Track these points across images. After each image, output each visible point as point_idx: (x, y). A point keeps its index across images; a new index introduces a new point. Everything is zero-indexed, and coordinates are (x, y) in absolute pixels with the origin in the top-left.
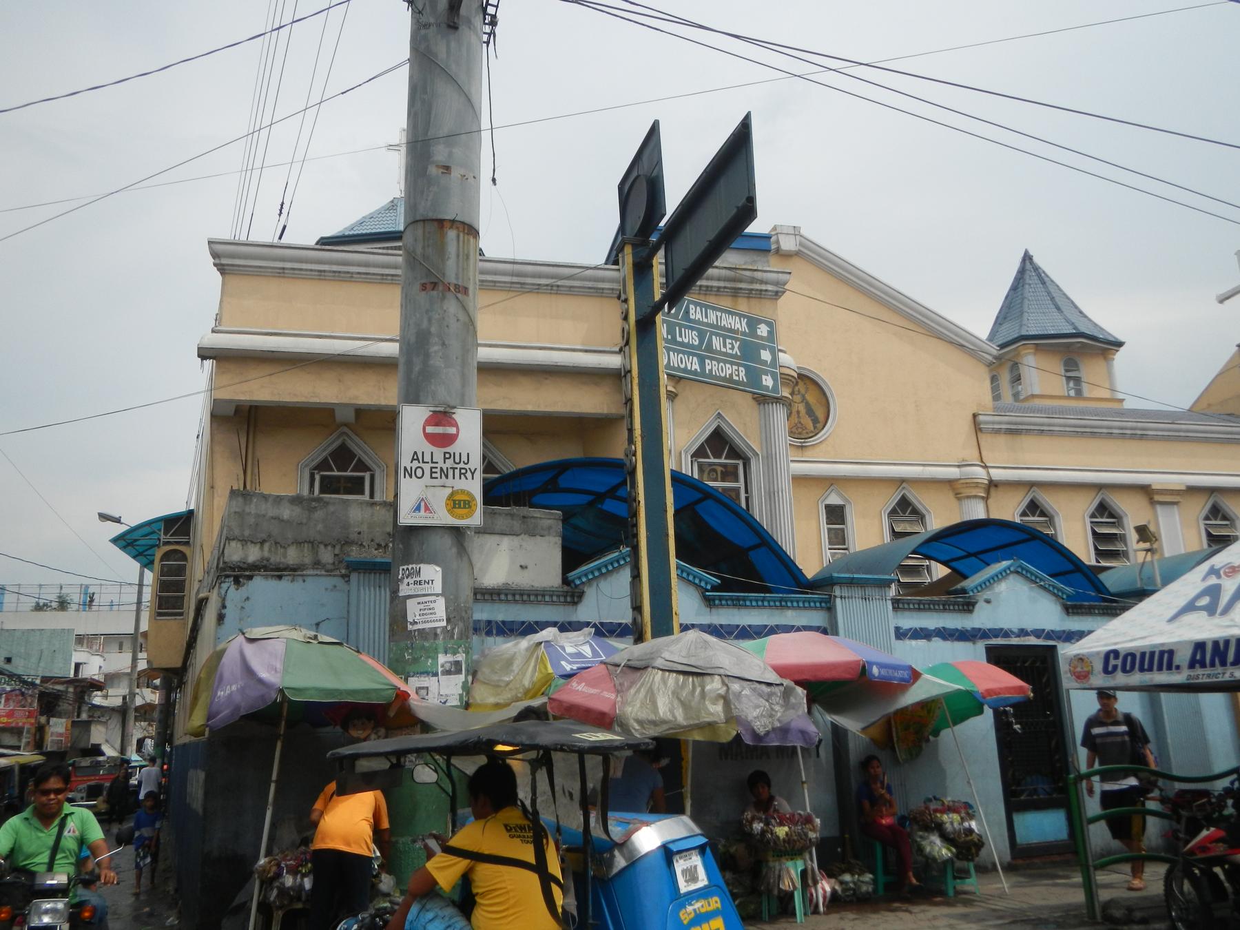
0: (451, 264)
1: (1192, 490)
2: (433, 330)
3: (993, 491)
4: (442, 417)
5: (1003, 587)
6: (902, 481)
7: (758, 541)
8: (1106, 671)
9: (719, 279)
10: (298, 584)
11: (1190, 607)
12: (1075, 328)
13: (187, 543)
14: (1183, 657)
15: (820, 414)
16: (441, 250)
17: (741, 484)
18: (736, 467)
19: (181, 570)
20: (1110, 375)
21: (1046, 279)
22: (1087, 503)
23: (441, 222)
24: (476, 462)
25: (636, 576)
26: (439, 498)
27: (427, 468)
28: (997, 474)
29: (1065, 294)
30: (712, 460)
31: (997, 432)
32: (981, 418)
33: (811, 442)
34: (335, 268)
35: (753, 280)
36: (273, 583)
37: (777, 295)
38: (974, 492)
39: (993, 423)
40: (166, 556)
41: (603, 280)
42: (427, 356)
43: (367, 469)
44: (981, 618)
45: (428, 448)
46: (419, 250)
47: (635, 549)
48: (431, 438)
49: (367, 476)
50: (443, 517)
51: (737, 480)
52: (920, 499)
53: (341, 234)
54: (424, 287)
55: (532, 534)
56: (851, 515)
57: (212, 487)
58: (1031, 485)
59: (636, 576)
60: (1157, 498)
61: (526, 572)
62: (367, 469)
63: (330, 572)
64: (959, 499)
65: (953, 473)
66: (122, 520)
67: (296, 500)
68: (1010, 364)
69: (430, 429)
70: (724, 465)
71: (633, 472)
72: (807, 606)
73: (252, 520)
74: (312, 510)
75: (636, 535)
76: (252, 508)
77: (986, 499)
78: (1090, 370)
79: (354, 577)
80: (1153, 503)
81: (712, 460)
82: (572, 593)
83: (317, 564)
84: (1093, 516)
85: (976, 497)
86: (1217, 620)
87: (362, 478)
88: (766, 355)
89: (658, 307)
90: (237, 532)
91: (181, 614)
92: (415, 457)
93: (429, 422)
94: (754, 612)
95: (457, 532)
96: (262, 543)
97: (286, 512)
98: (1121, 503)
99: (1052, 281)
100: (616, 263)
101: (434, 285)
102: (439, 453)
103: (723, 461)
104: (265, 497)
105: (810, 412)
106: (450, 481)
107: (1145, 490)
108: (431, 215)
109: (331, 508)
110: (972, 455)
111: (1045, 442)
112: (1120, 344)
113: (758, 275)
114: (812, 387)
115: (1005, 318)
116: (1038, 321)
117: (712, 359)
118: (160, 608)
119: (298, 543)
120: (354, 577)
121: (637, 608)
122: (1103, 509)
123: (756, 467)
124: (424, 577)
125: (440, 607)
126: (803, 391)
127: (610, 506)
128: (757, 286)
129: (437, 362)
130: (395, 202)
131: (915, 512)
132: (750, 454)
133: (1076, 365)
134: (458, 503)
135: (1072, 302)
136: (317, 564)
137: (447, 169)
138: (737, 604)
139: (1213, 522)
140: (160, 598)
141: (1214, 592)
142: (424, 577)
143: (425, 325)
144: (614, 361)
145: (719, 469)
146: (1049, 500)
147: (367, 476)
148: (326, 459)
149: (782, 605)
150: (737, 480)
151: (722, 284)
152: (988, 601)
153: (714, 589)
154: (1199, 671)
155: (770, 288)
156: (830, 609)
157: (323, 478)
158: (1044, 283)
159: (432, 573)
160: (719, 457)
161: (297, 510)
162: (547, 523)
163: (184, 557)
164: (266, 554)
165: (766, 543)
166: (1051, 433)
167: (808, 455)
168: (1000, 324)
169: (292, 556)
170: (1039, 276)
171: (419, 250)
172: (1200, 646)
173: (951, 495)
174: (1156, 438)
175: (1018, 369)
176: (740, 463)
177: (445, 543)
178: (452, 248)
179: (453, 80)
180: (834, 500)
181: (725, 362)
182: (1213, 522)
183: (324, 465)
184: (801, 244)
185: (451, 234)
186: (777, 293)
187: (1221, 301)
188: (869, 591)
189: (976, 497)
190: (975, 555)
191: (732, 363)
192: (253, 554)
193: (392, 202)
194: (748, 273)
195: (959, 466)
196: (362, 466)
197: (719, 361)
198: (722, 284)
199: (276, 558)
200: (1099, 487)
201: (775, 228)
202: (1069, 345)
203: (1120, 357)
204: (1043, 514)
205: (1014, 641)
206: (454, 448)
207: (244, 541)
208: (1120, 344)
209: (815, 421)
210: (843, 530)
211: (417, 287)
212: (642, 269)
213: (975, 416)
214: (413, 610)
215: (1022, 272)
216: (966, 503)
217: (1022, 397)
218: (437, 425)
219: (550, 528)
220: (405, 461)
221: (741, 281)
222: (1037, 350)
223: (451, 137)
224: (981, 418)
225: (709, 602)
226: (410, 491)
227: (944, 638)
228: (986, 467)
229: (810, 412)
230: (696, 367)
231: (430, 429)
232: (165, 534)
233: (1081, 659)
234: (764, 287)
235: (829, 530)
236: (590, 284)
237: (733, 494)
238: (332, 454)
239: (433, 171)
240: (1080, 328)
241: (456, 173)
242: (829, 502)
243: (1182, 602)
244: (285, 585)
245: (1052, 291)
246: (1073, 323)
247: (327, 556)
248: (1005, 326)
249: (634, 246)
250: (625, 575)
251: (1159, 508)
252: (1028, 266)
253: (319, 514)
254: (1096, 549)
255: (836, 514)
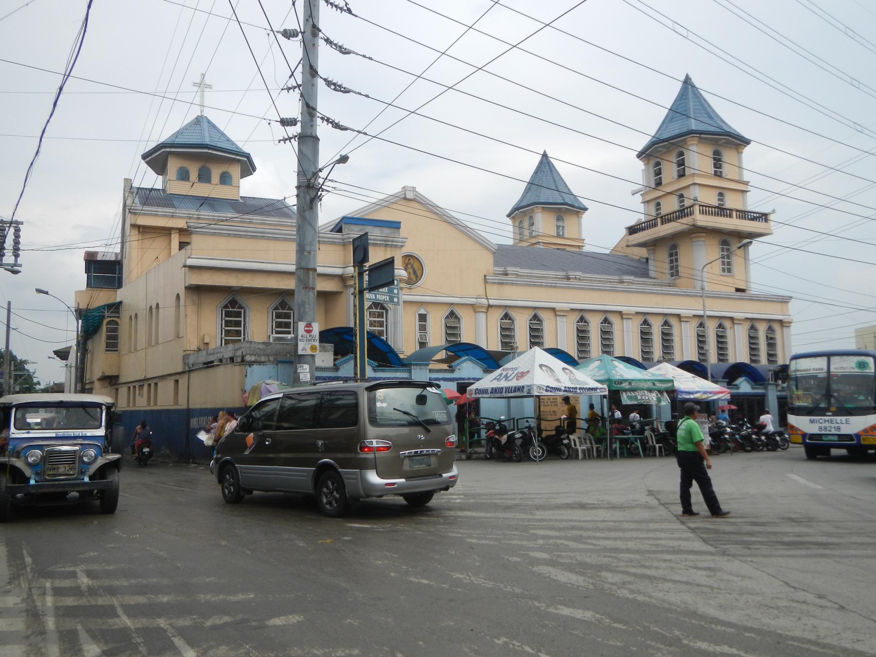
0: (311, 282)
1: (572, 310)
2: (306, 300)
3: (490, 308)
4: (309, 325)
5: (464, 365)
6: (452, 304)
7: (389, 350)
8: (475, 393)
9: (380, 241)
10: (265, 366)
11: (495, 379)
12: (563, 200)
13: (118, 317)
14: (489, 391)
15: (419, 275)
16: (308, 278)
17: (384, 319)
18: (383, 313)
19: (116, 330)
20: (579, 225)
21: (553, 170)
22: (528, 315)
23: (308, 269)
24: (317, 337)
25: (356, 365)
26: (308, 347)
27: (305, 339)
28: (492, 302)
29: (562, 178)
30: (375, 310)
31: (495, 283)
32: (488, 277)
33: (413, 286)
34: (235, 233)
35: (393, 241)
36: (258, 366)
37: (402, 246)
38: (482, 310)
39: (493, 279)
40: (108, 323)
41: (336, 238)
42: (305, 308)
43: (242, 308)
44: (456, 375)
45: (305, 334)
46: (302, 277)
47: (356, 357)
48: (306, 331)
49: (242, 311)
50: (309, 352)
51: (383, 318)
52: (459, 312)
53: (170, 141)
54: (303, 288)
55: (326, 351)
56: (429, 318)
57: (186, 315)
58: (506, 307)
59: (356, 365)
60: (558, 313)
61: (324, 363)
62: (242, 308)
63: (273, 363)
64: (475, 312)
65: (473, 301)
66: (49, 293)
67: (263, 343)
68: (530, 215)
69: (306, 329)
70: (379, 312)
71: (356, 336)
72: (403, 371)
73: (252, 349)
74: (268, 346)
75: (356, 354)
76: (252, 346)
77: (486, 313)
78: (569, 223)
79: (279, 365)
80: (556, 315)
81: (375, 310)
82: (336, 368)
83: (269, 361)
84: (531, 320)
85: (482, 312)
86: (499, 383)
87: (241, 312)
88: (395, 291)
89: (365, 289)
90: (249, 352)
91: (117, 351)
92: (302, 336)
93: (306, 327)
94: (387, 373)
95: (313, 356)
96: (255, 355)
97: (261, 347)
98: (542, 315)
99: (556, 170)
100: (340, 230)
101: (306, 288)
102: (308, 335)
103: (378, 310)
104: (255, 343)
105: (415, 273)
106: (311, 343)
107: (553, 310)
108: (305, 267)
109: (272, 345)
110: (482, 292)
111: (514, 287)
112: (586, 209)
113: (395, 239)
114: (416, 261)
115: (529, 189)
116: (546, 196)
117: (378, 294)
118: (107, 347)
119: (264, 355)
120: (279, 365)
121: (356, 374)
122: (535, 317)
123: (391, 314)
124: (304, 368)
125: (308, 375)
126: (412, 263)
127: (345, 336)
128: (395, 244)
129: (307, 310)
130: (199, 118)
131: (456, 317)
132: (388, 308)
133: (563, 220)
134: (313, 348)
135: (565, 183)
136: (269, 361)
137: (310, 253)
138: (383, 371)
139: (581, 324)
140: (107, 343)
141: (501, 375)
142: (304, 368)
143: (304, 299)
144: (339, 271)
145: (377, 313)
146: (513, 314)
147: (242, 311)
148: (227, 304)
149: (396, 371)
150: (383, 318)
151: (381, 242)
152: (459, 369)
153: (377, 366)
154: (492, 395)
155: (399, 244)
156: (410, 372)
157: (226, 311)
158: (551, 171)
159: (306, 367)
160: (377, 309)
161: (264, 346)
162: (329, 348)
163: (117, 324)
164: (256, 358)
165: (391, 351)
166: (517, 284)
167: (413, 292)
168: (527, 193)
169: (263, 359)
170: (549, 166)
171: (302, 277)
172: (493, 389)
173: (472, 310)
174: (561, 287)
175: (533, 219)
176: (384, 311)
177: (310, 359)
178: (311, 277)
179: (311, 225)
180: (422, 312)
181: (383, 295)
182: (581, 324)
183: (226, 306)
184: (415, 195)
185: (311, 273)
186: (402, 246)
187: (633, 194)
188: (422, 367)
189: (482, 312)
190: (463, 351)
191: (385, 295)
192: (253, 358)
193: (197, 118)
194: (391, 239)
195: (476, 298)
196: (241, 307)
197: (381, 295)
198: (381, 242)
199: (259, 359)
200: (535, 308)
201: (404, 187)
202: (559, 209)
203: (585, 216)
204: (510, 319)
205: (466, 381)
206: (312, 333)
207: (251, 355)
208: (586, 209)
209: (417, 277)
210: (425, 325)
211: (301, 288)
212: (361, 274)
213: (485, 276)
214: (301, 376)
215: (541, 163)
216: (477, 314)
217: (534, 234)
218: (308, 327)
219: (330, 349)
220: (299, 337)
221: (389, 241)
222: (543, 210)
223: (311, 244)
224: (488, 277)
225: (375, 371)
226: (301, 345)
227: (444, 381)
228: (487, 299)
229: (415, 273)
230: (374, 297)
231: (306, 329)
232: (108, 312)
233: (471, 390)
234: (397, 244)
235: (419, 325)
236: (331, 240)
237: (381, 323)
238: (229, 302)
239: (306, 253)
240: (565, 199)
241: (312, 253)
242: (420, 312)
243: (494, 377)
244: (261, 366)
245: (555, 176)
246: (563, 197)
247: (271, 358)
248: (529, 194)
249: (359, 267)
250: (352, 363)
251: (558, 317)
252: (545, 161)
253: (270, 347)
254: (530, 334)
255: (423, 318)
